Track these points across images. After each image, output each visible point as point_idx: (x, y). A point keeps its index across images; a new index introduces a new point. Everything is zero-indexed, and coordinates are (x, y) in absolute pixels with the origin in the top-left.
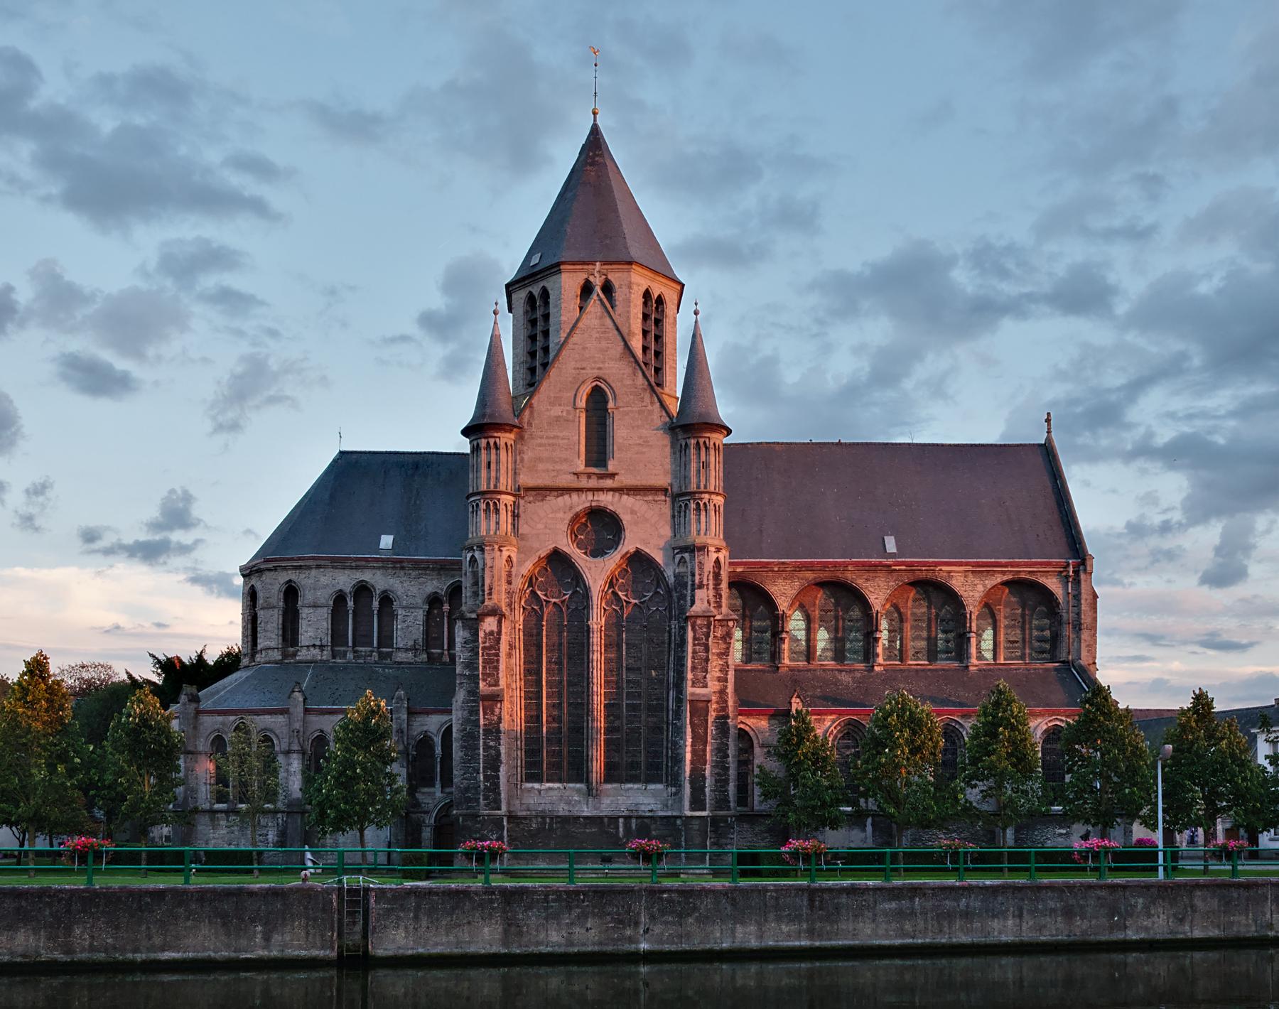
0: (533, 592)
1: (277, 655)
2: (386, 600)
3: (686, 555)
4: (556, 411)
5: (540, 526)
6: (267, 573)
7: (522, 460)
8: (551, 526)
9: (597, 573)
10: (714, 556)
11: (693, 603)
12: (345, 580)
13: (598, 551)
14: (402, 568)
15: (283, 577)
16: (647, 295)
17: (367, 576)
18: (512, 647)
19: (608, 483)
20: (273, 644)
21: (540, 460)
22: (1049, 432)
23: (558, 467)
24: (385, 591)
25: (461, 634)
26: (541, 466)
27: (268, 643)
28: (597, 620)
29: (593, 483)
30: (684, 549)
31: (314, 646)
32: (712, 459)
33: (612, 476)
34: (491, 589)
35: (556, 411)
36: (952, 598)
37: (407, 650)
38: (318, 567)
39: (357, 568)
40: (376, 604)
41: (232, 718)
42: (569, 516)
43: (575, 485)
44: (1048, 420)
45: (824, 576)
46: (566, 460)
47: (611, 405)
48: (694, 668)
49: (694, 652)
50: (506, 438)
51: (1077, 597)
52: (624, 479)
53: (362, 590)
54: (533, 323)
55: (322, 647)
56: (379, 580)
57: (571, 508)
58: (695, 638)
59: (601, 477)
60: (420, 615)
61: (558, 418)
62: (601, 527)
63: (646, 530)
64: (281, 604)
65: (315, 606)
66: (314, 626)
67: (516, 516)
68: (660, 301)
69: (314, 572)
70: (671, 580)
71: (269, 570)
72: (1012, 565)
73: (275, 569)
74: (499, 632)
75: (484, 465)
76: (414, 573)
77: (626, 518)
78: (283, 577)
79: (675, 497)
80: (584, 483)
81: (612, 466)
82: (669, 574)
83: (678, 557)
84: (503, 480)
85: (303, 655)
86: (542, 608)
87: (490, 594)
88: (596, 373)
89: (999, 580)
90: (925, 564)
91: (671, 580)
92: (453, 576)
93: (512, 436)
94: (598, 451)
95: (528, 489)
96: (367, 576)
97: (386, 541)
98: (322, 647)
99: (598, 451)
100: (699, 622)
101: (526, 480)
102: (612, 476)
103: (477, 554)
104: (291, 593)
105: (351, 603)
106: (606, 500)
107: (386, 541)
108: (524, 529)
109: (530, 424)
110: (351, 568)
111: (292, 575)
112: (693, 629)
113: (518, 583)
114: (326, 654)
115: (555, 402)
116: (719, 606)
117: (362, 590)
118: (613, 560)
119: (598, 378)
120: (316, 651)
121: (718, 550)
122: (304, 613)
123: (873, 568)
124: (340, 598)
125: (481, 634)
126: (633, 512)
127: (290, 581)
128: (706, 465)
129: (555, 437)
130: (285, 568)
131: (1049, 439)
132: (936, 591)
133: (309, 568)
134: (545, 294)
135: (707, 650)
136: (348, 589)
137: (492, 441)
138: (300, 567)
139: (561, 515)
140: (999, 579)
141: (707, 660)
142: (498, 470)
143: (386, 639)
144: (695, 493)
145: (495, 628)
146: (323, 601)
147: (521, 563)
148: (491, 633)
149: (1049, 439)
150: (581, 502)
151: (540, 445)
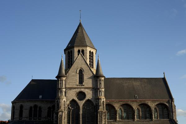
0: (69, 108)
1: (18, 119)
2: (40, 108)
4: (73, 74)
5: (70, 95)
6: (17, 103)
7: (67, 82)
8: (73, 95)
9: (81, 103)
10: (103, 100)
11: (99, 109)
12: (32, 104)
13: (81, 99)
14: (44, 102)
15: (20, 104)
16: (90, 52)
17: (36, 103)
18: (64, 118)
19: (83, 87)
20: (17, 117)
21: (70, 82)
22: (164, 76)
23: (74, 84)
24: (40, 107)
25: (55, 115)
26: (70, 84)
27: (16, 117)
28: (81, 112)
29: (80, 87)
30: (97, 99)
31: (26, 117)
32: (102, 82)
33: (84, 85)
34: (61, 107)
35: (73, 74)
36: (149, 107)
37: (44, 118)
38: (27, 102)
39: (34, 102)
40: (38, 109)
42: (75, 93)
43: (77, 87)
44: (164, 74)
45: (124, 103)
46: (75, 82)
47: (83, 72)
48: (99, 122)
49: (99, 118)
50: (64, 79)
51: (172, 106)
52: (86, 86)
53: (36, 106)
54: (69, 56)
55: (27, 118)
56: (39, 104)
57: (76, 91)
58: (99, 116)
59: (82, 86)
60: (46, 111)
61: (73, 75)
62: (81, 95)
63: (89, 95)
64: (19, 109)
65: (26, 109)
66: (26, 113)
67: (65, 93)
68: (92, 53)
69: (26, 103)
70: (95, 104)
71: (17, 102)
72: (160, 100)
73: (19, 102)
74: (62, 115)
75: (60, 83)
76: (46, 103)
77: (86, 93)
78: (20, 104)
79: (95, 89)
80: (78, 87)
81: (84, 84)
82: (94, 103)
84: (63, 86)
85: (23, 119)
86: (70, 110)
87: (60, 108)
88: (80, 67)
89: (157, 103)
90: (143, 100)
91: (95, 104)
93: (65, 78)
94: (81, 81)
95: (68, 88)
96: (36, 103)
97: (41, 97)
98: (27, 118)
99: (81, 81)
100: (100, 112)
101: (67, 86)
102: (84, 85)
103: (58, 100)
104: (21, 107)
105: (33, 109)
106: (82, 90)
107: (41, 97)
108: (67, 95)
109: (68, 76)
110: (33, 102)
111: (22, 103)
112: (99, 114)
113: (66, 106)
114: (28, 119)
115: (73, 72)
116: (104, 109)
117: (36, 106)
118: (84, 102)
119: (81, 68)
121: (103, 99)
122: (24, 111)
123: (133, 101)
124: (31, 108)
125: (59, 115)
126: (87, 92)
128: (101, 83)
129: (73, 78)
130: (20, 102)
131: (164, 77)
132: (145, 106)
133: (25, 102)
134: (71, 51)
135: (102, 118)
137: (61, 79)
138: (23, 102)
139: (74, 93)
140: (157, 103)
141: (102, 120)
142: (62, 84)
143: (40, 116)
144: (99, 89)
145: (61, 114)
147: (66, 102)
148: (61, 115)
149: (164, 77)
150: (78, 90)
151: (71, 80)
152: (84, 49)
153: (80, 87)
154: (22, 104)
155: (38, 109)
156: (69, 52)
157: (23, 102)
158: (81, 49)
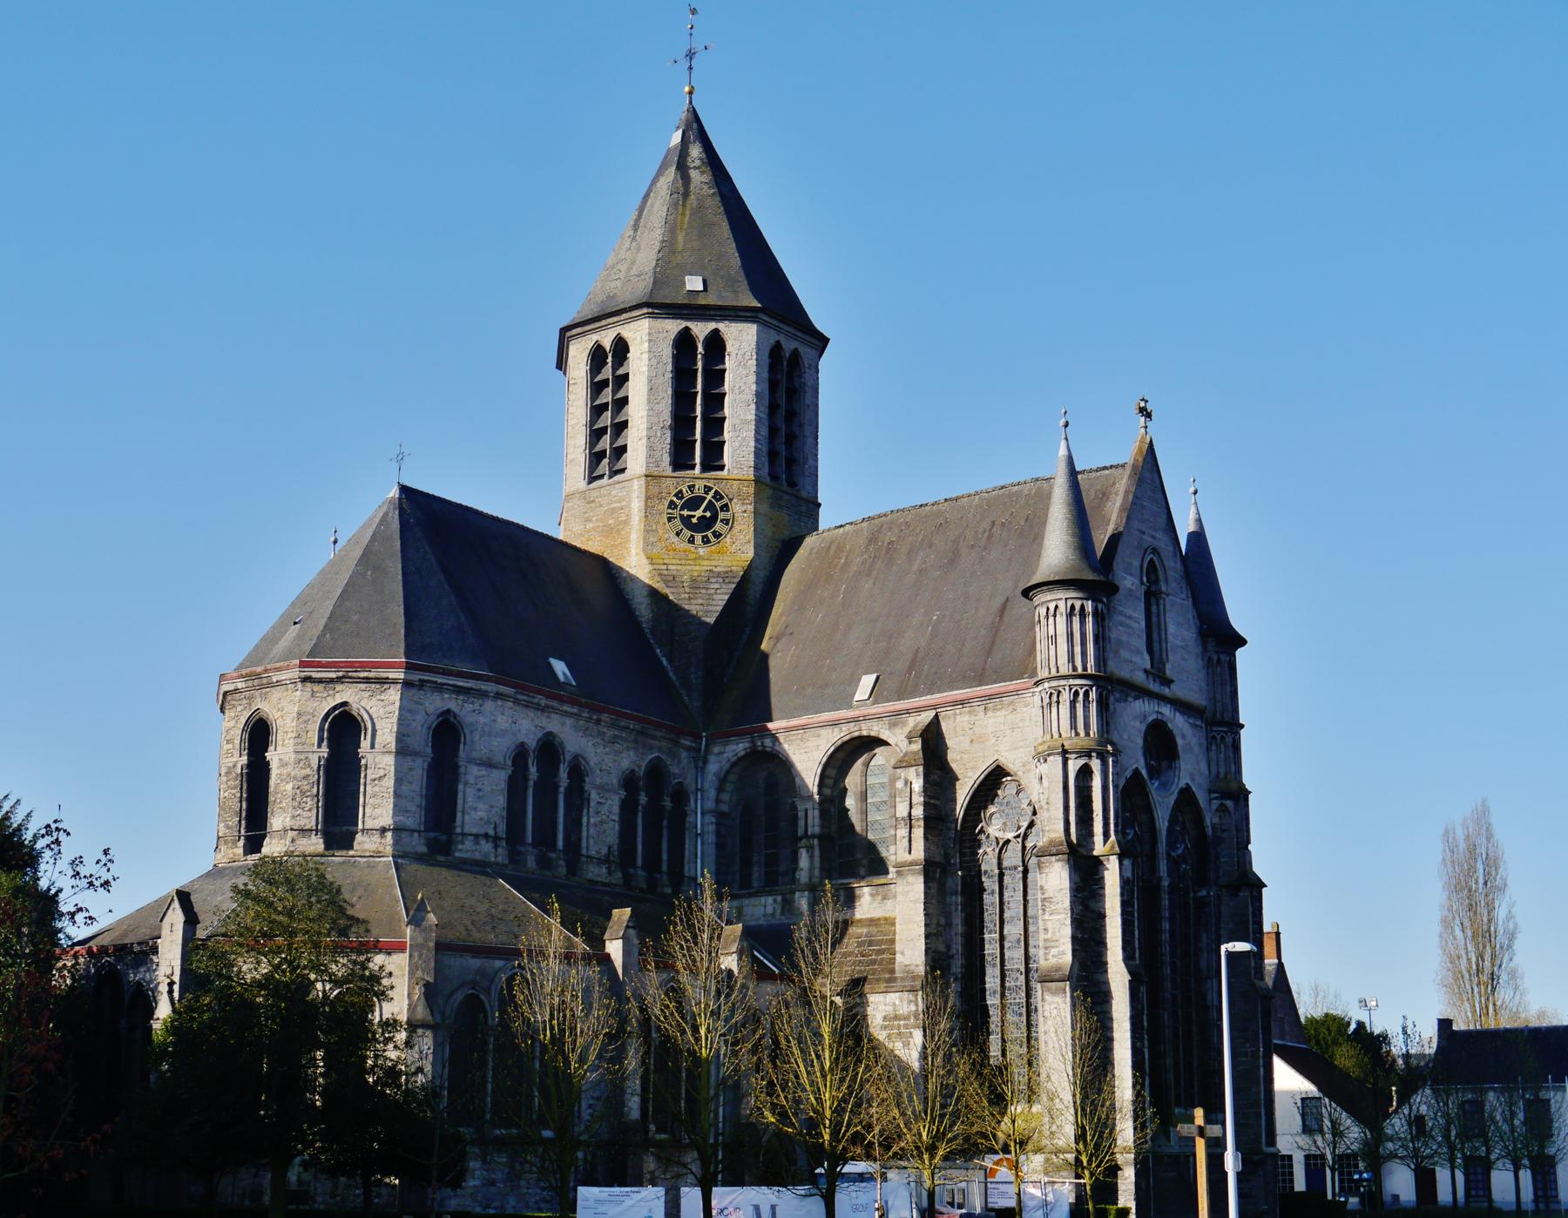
2: (578, 771)
3: (1229, 803)
24: (576, 757)
31: (486, 836)
40: (563, 774)
41: (498, 964)
42: (1143, 728)
53: (549, 748)
65: (490, 764)
69: (489, 705)
70: (1209, 831)
76: (610, 733)
83: (1216, 803)
92: (651, 748)
98: (496, 839)
111: (451, 703)
117: (549, 748)
120: (486, 847)
124: (520, 755)
126: (1184, 737)
127: (448, 711)
130: (439, 688)
136: (532, 743)
146: (499, 758)
151: (1122, 624)
152: (805, 351)
153: (1154, 686)
154: (452, 706)
155: (563, 774)
156: (684, 343)
157: (459, 691)
158: (789, 346)
